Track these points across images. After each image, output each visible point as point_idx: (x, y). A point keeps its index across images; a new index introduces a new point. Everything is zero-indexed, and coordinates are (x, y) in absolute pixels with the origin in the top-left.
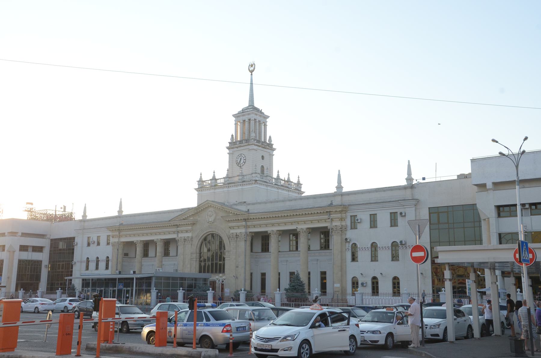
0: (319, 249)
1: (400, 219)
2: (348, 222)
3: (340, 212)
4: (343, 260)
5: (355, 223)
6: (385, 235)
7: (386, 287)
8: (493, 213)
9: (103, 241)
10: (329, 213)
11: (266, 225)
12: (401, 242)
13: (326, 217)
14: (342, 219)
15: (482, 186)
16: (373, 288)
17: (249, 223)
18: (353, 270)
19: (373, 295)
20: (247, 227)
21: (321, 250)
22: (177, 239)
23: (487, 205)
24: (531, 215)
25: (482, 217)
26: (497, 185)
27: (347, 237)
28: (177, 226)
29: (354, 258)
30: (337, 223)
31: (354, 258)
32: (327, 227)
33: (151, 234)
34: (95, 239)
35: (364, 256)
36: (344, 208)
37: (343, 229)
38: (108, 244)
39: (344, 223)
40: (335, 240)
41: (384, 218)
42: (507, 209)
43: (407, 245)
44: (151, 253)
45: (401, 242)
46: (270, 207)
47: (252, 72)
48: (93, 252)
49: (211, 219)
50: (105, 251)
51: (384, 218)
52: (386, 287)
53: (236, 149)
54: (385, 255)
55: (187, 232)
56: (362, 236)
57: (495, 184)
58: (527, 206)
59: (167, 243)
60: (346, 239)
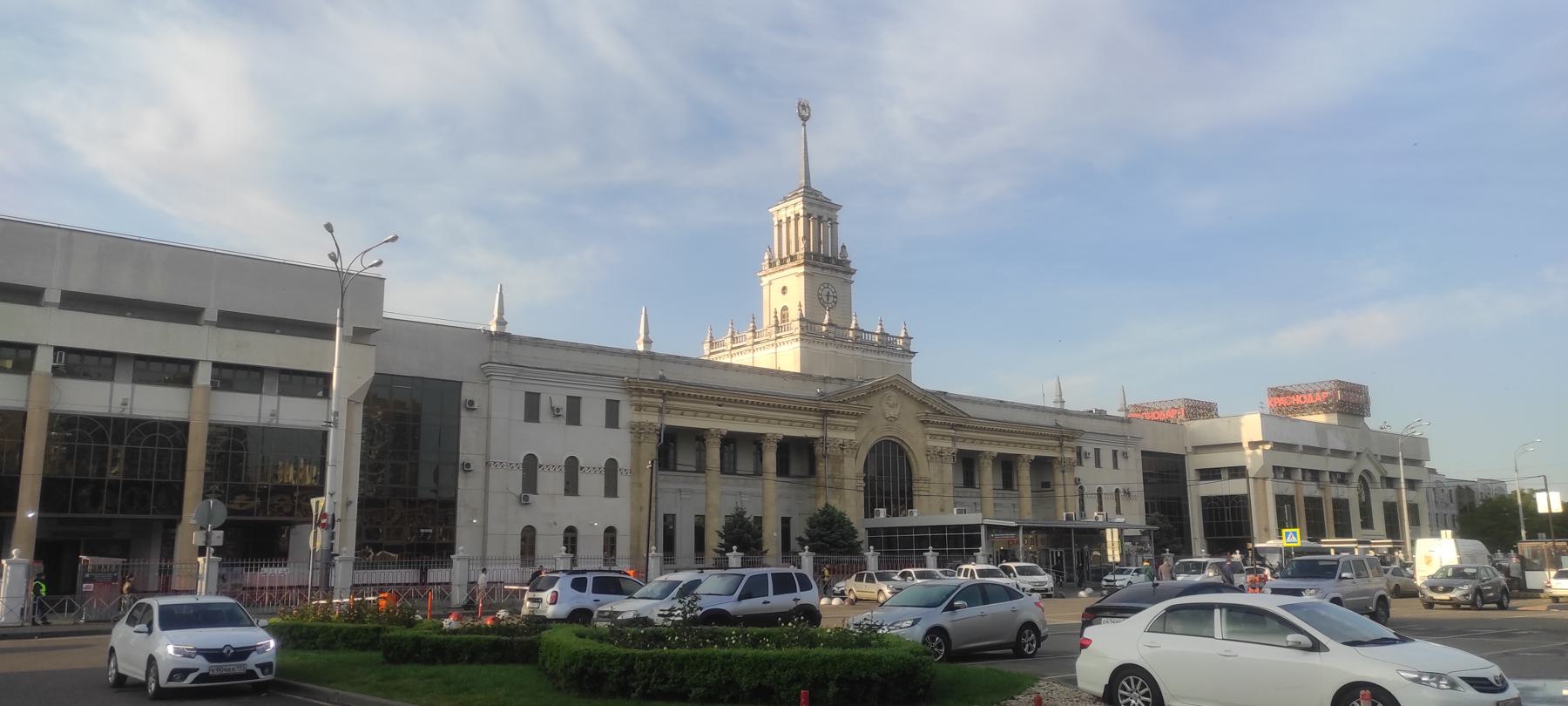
9: (593, 411)
11: (982, 441)
17: (959, 433)
20: (954, 439)
22: (824, 441)
28: (826, 413)
33: (757, 419)
34: (561, 403)
38: (612, 420)
44: (686, 458)
47: (804, 119)
48: (551, 442)
49: (892, 412)
50: (596, 443)
53: (818, 270)
55: (846, 428)
59: (786, 447)
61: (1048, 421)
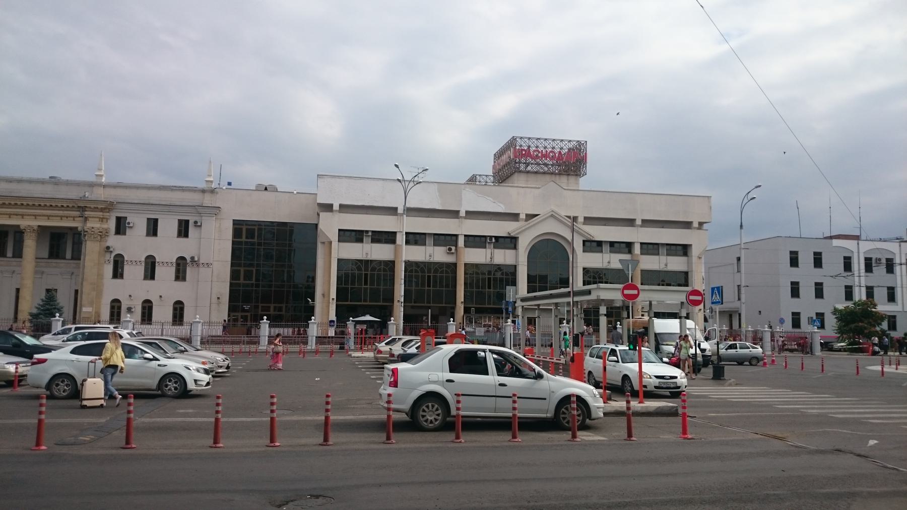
0: (47, 256)
1: (192, 230)
2: (112, 224)
3: (102, 210)
4: (100, 276)
5: (121, 227)
6: (167, 247)
7: (163, 313)
8: (334, 237)
10: (83, 209)
12: (192, 258)
13: (78, 213)
14: (102, 220)
15: (328, 208)
16: (112, 314)
18: (112, 289)
19: (173, 325)
21: (49, 258)
23: (330, 226)
24: (668, 255)
25: (320, 239)
26: (344, 208)
27: (108, 244)
29: (118, 273)
30: (93, 224)
31: (118, 273)
32: (77, 228)
35: (134, 272)
36: (109, 207)
37: (103, 235)
39: (105, 226)
40: (91, 249)
41: (168, 226)
42: (348, 233)
43: (201, 261)
45: (192, 258)
46: (48, 191)
51: (168, 226)
52: (163, 313)
54: (165, 273)
56: (134, 246)
57: (341, 206)
58: (370, 234)
60: (108, 248)
61: (73, 194)
